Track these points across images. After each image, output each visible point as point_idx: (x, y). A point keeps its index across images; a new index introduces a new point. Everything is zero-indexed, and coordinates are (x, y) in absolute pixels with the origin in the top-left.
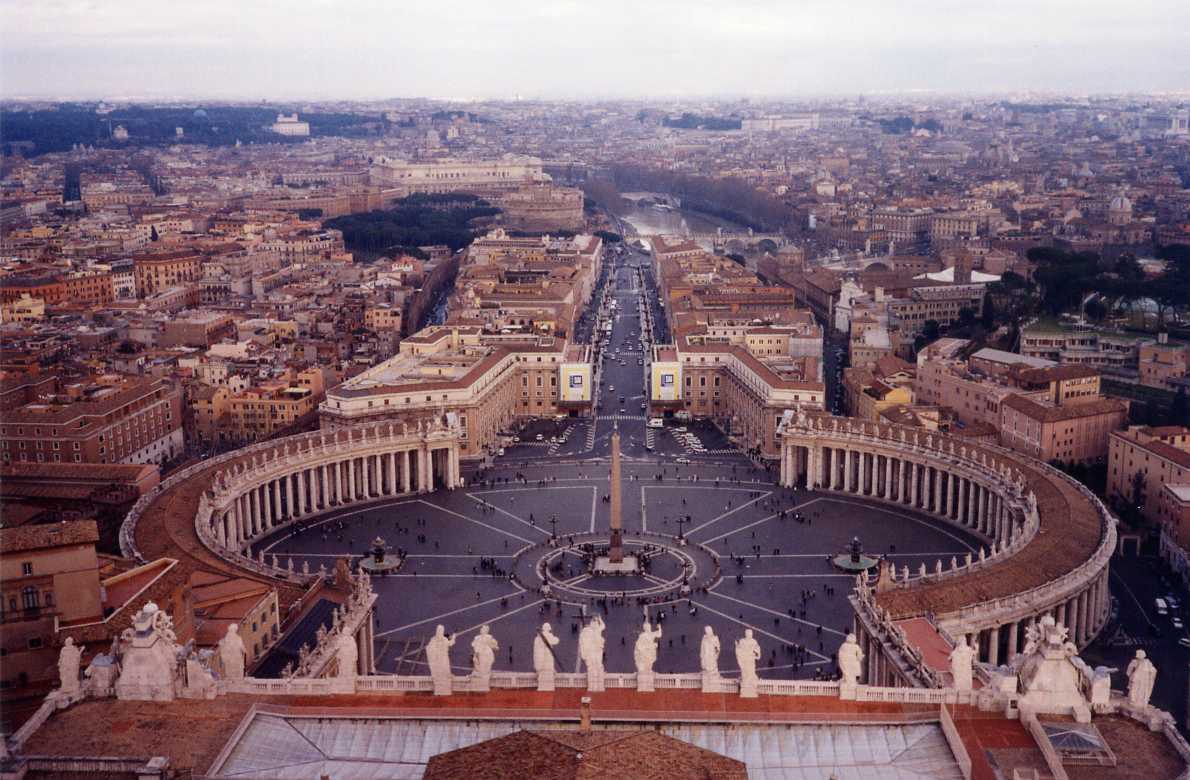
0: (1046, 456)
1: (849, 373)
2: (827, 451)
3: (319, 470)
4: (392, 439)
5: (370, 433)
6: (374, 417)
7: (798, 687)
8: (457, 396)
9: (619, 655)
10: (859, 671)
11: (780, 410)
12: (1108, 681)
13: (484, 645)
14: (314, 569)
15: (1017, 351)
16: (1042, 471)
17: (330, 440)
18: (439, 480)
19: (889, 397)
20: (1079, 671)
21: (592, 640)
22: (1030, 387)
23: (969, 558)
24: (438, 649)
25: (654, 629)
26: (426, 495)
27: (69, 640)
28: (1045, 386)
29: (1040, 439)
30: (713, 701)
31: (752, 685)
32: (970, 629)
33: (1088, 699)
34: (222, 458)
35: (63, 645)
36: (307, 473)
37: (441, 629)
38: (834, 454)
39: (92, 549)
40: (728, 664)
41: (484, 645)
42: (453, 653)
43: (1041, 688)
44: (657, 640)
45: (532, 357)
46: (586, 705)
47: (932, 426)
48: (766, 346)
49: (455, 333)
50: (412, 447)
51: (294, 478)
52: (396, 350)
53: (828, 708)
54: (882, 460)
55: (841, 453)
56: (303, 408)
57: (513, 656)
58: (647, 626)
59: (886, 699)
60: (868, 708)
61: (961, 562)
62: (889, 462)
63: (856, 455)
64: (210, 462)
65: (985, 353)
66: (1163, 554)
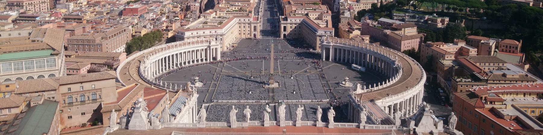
0: (402, 51)
1: (340, 25)
2: (336, 50)
3: (177, 55)
4: (200, 45)
5: (193, 43)
6: (193, 37)
7: (347, 125)
8: (219, 31)
9: (291, 115)
10: (366, 120)
11: (320, 36)
12: (442, 122)
13: (248, 112)
14: (178, 86)
15: (391, 18)
16: (402, 56)
17: (180, 45)
18: (215, 59)
19: (354, 32)
20: (434, 119)
21: (282, 111)
22: (396, 29)
23: (384, 83)
24: (233, 113)
25: (301, 107)
26: (211, 63)
27: (114, 110)
28: (400, 30)
29: (400, 46)
30: (320, 130)
31: (332, 124)
32: (384, 104)
33: (436, 128)
34: (146, 51)
35: (111, 111)
36: (173, 56)
37: (234, 107)
38: (338, 50)
39: (115, 80)
40: (325, 119)
41: (248, 112)
42: (237, 114)
43: (422, 124)
44: (302, 110)
45: (242, 20)
46: (283, 132)
47: (368, 42)
48: (315, 17)
49: (218, 12)
50: (206, 47)
51: (169, 57)
52: (199, 17)
53: (358, 132)
54: (353, 52)
55: (340, 50)
56: (170, 35)
57: (258, 115)
58: (300, 106)
59: (374, 128)
60: (369, 131)
61: (381, 84)
62: (355, 53)
63: (345, 50)
64: (142, 53)
65: (382, 19)
66: (438, 81)
